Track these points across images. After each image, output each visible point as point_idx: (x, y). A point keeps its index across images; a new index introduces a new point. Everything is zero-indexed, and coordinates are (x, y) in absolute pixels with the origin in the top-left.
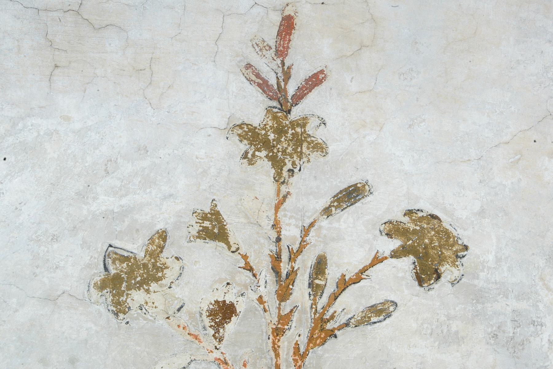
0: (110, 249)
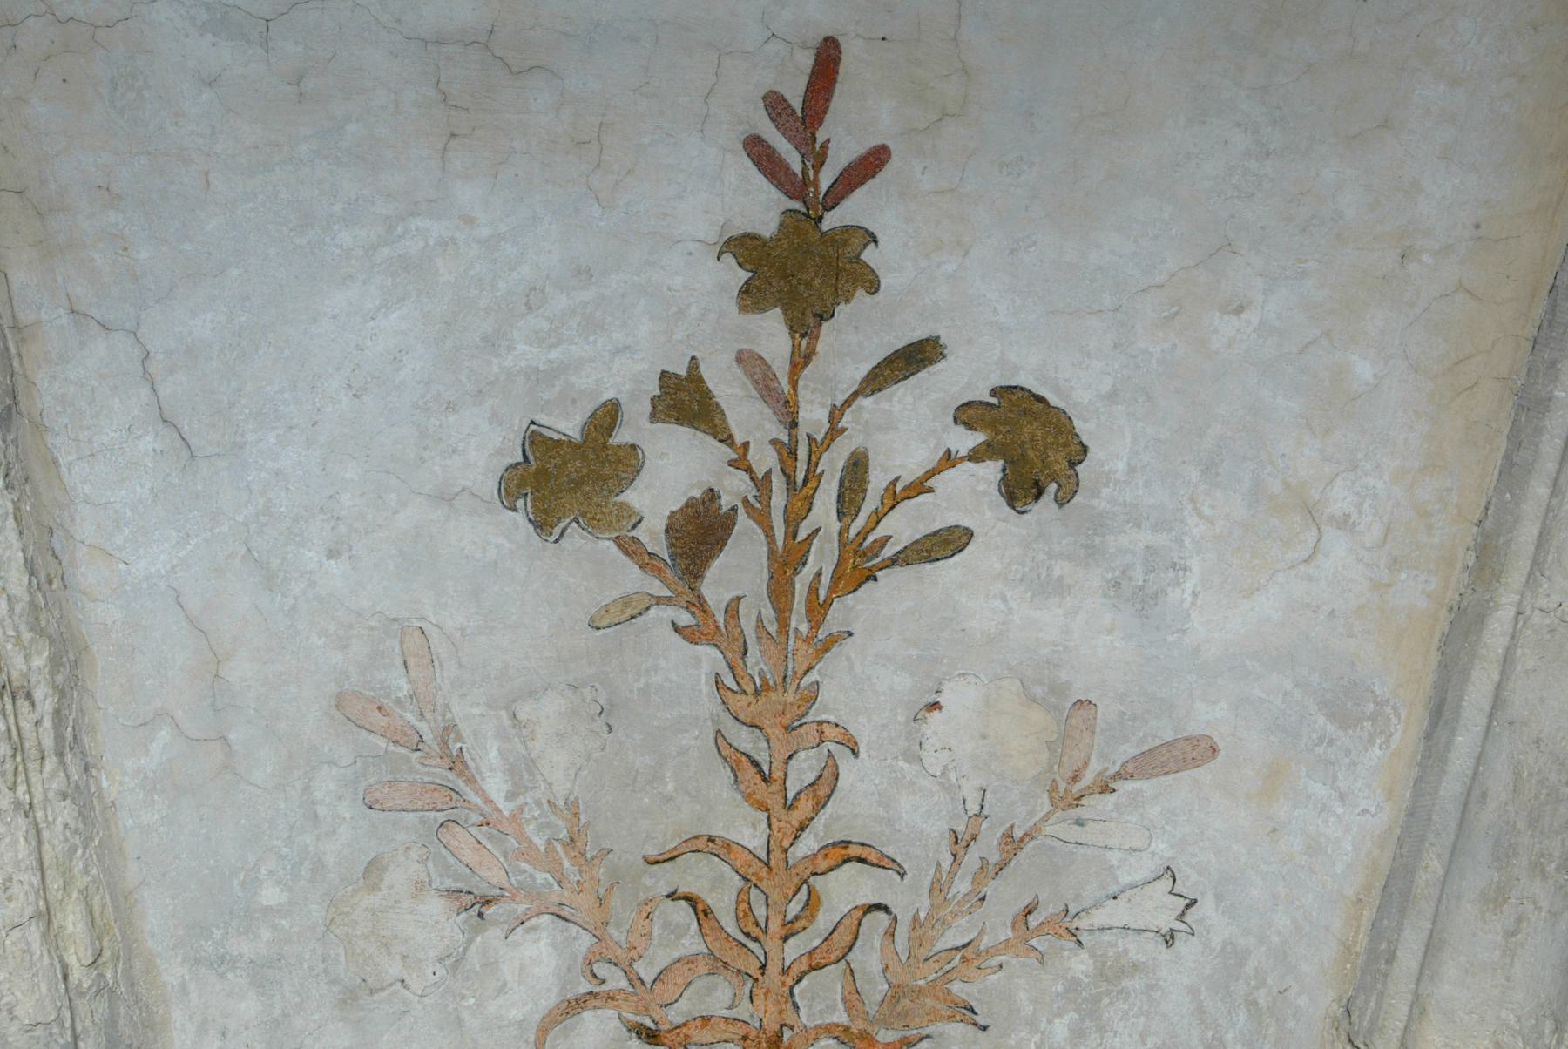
0: (533, 427)
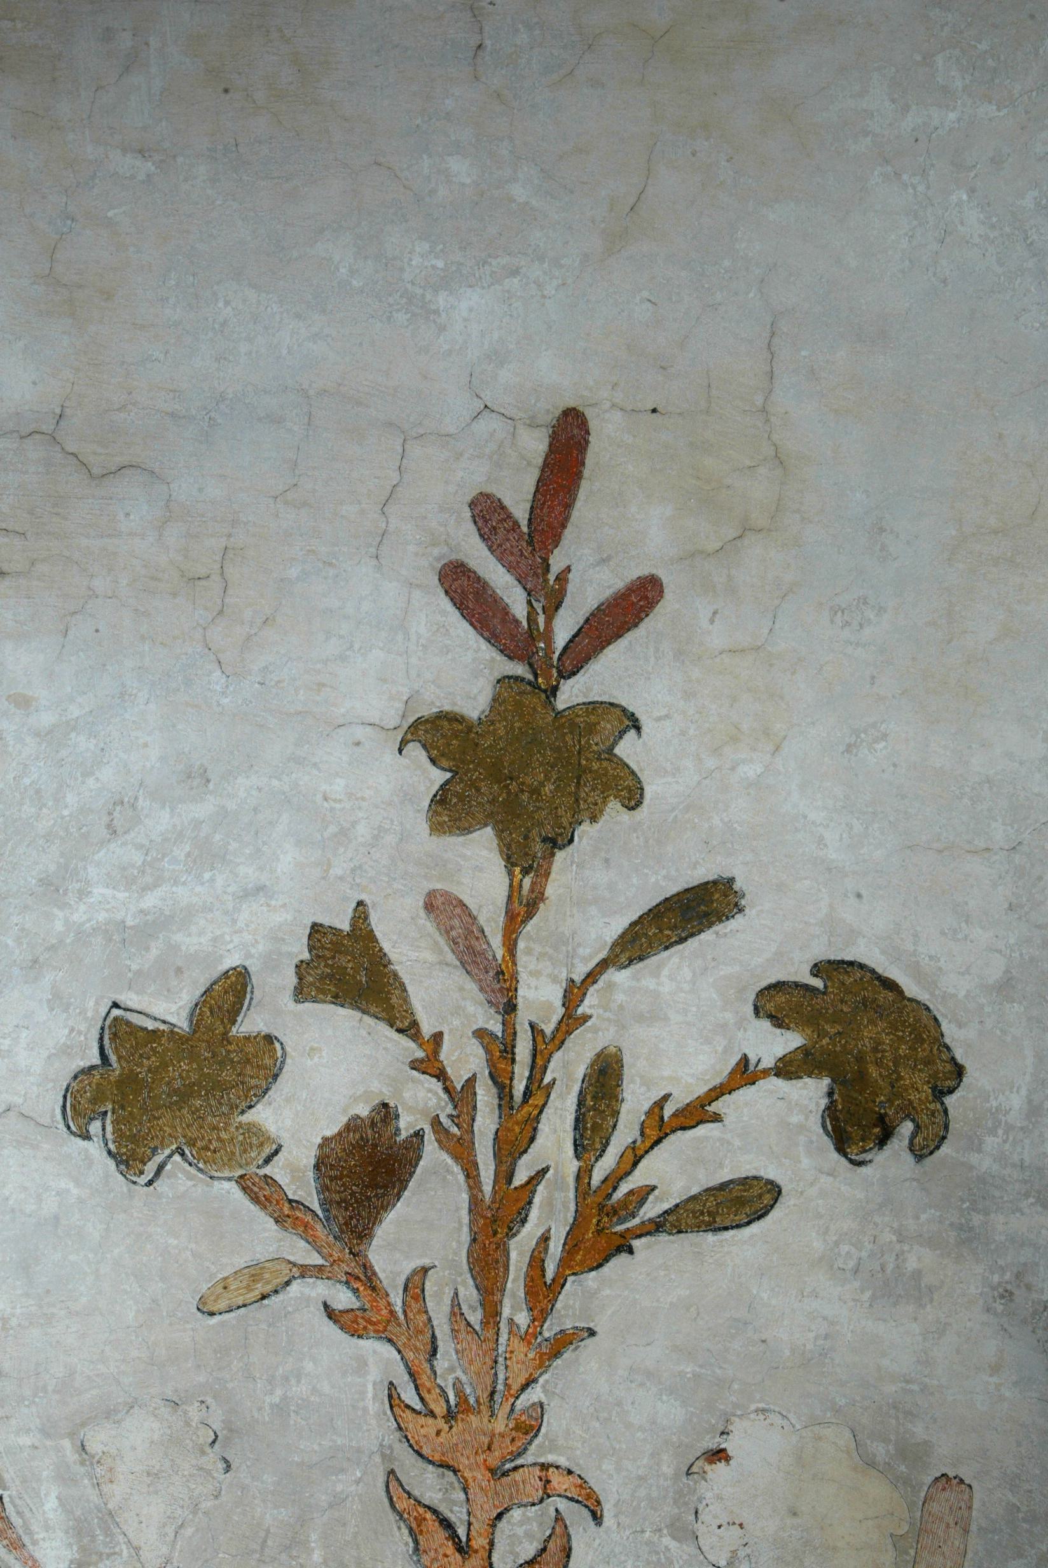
0: (116, 1012)
